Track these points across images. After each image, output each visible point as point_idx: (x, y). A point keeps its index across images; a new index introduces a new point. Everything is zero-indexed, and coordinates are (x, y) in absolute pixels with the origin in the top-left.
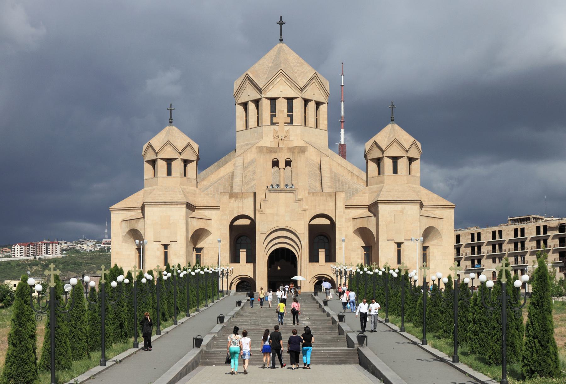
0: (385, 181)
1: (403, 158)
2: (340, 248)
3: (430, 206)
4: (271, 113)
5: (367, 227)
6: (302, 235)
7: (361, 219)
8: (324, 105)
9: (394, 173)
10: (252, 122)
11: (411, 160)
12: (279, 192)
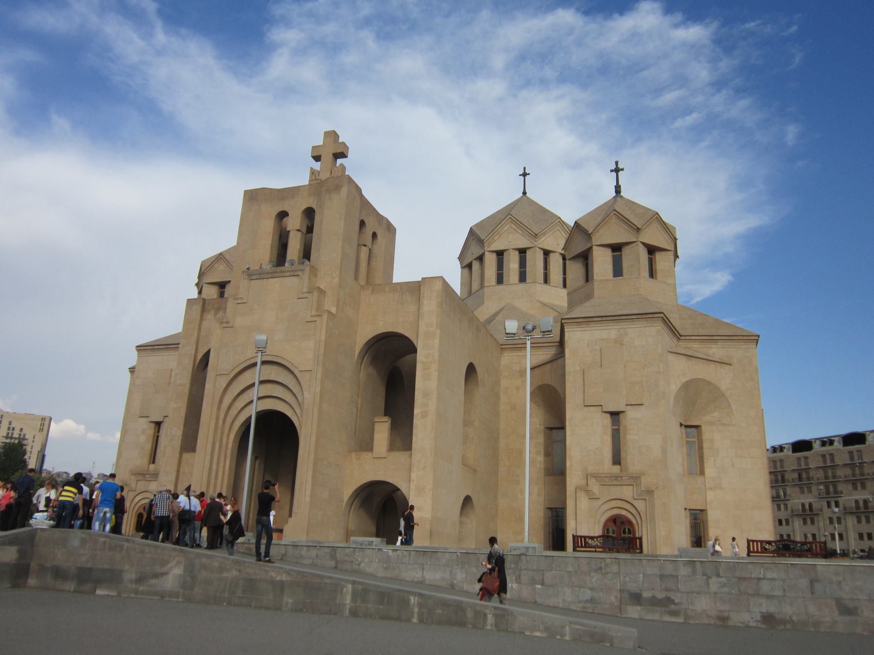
0: (595, 291)
1: (633, 245)
2: (424, 415)
3: (698, 338)
7: (541, 368)
9: (614, 277)
10: (475, 286)
11: (652, 250)
12: (269, 276)
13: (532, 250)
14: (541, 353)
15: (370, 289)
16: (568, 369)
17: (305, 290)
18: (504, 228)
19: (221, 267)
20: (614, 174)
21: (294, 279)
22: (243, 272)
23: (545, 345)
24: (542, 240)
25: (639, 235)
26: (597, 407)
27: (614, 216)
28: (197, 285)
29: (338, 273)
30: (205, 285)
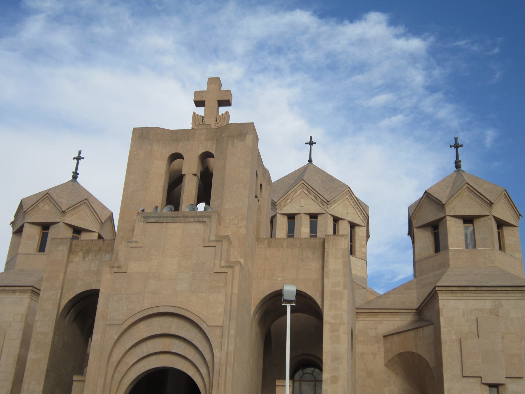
0: (451, 261)
1: (486, 218)
2: (335, 380)
4: (288, 234)
5: (415, 351)
6: (218, 331)
7: (402, 335)
8: (361, 228)
12: (169, 220)
13: (323, 216)
14: (398, 319)
15: (266, 242)
16: (444, 337)
17: (213, 238)
18: (296, 193)
19: (46, 207)
20: (454, 149)
21: (199, 226)
22: (138, 214)
23: (402, 311)
24: (333, 207)
25: (491, 209)
26: (476, 378)
27: (467, 189)
28: (13, 224)
29: (245, 223)
30: (26, 225)
